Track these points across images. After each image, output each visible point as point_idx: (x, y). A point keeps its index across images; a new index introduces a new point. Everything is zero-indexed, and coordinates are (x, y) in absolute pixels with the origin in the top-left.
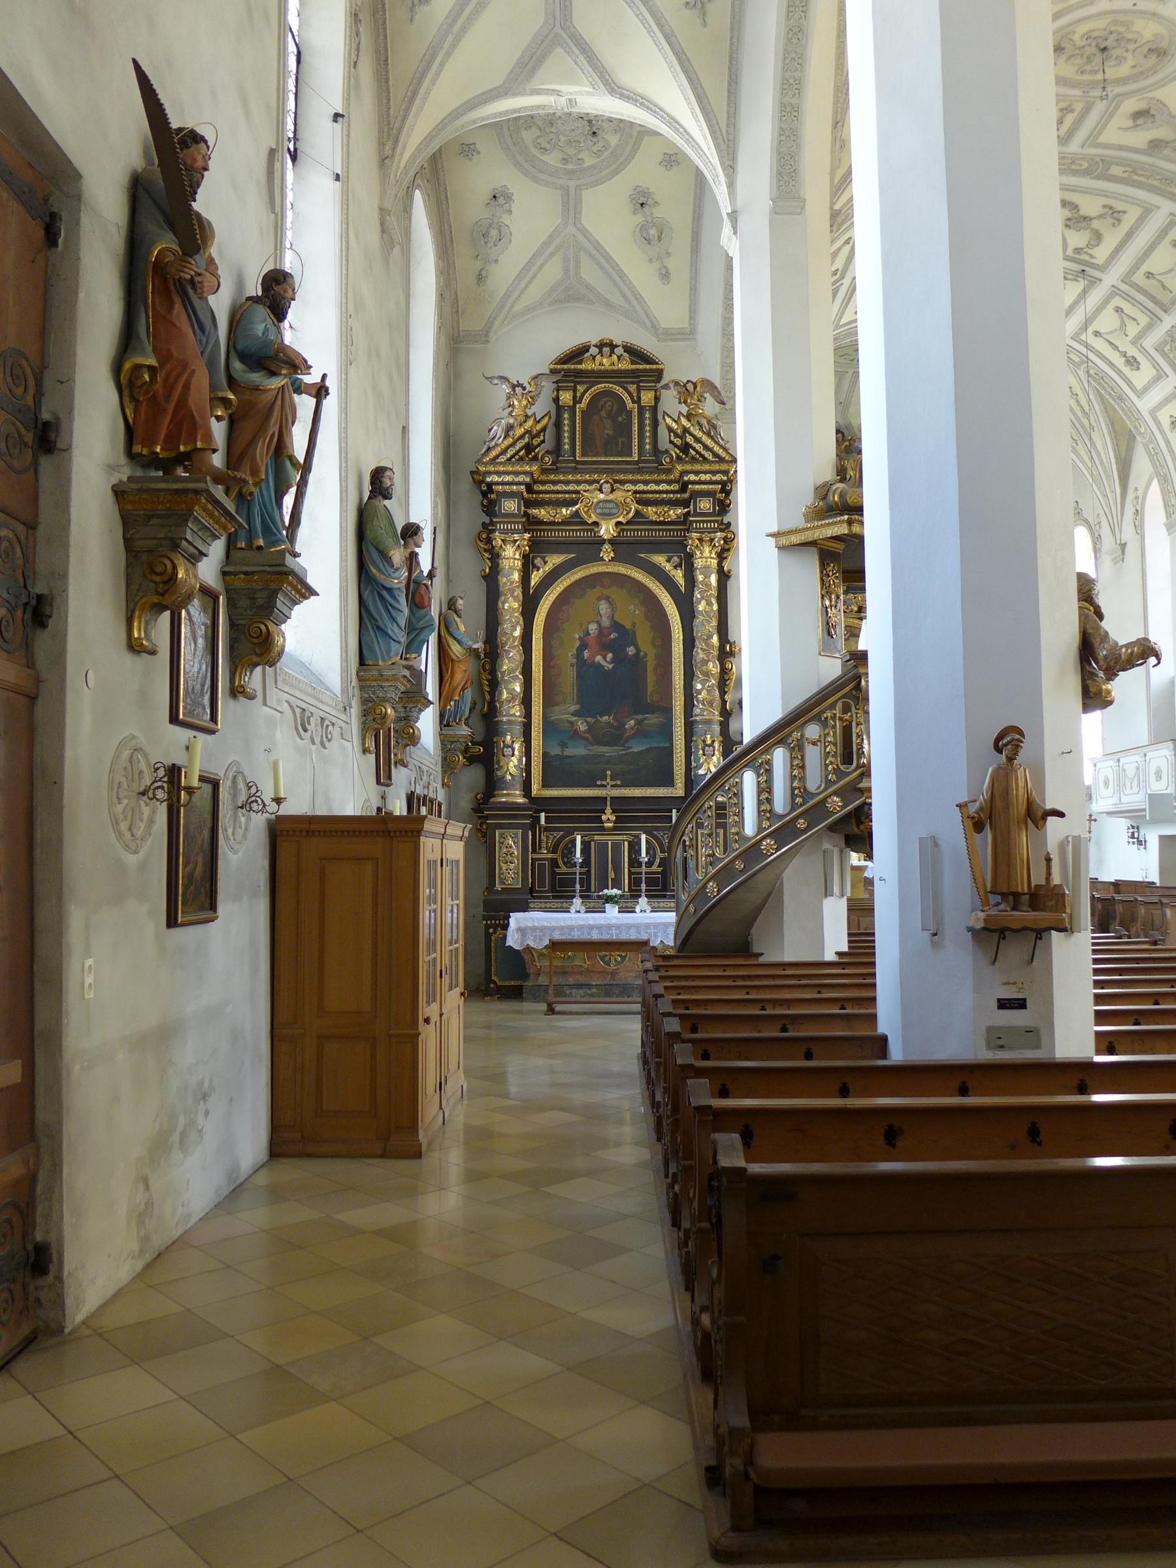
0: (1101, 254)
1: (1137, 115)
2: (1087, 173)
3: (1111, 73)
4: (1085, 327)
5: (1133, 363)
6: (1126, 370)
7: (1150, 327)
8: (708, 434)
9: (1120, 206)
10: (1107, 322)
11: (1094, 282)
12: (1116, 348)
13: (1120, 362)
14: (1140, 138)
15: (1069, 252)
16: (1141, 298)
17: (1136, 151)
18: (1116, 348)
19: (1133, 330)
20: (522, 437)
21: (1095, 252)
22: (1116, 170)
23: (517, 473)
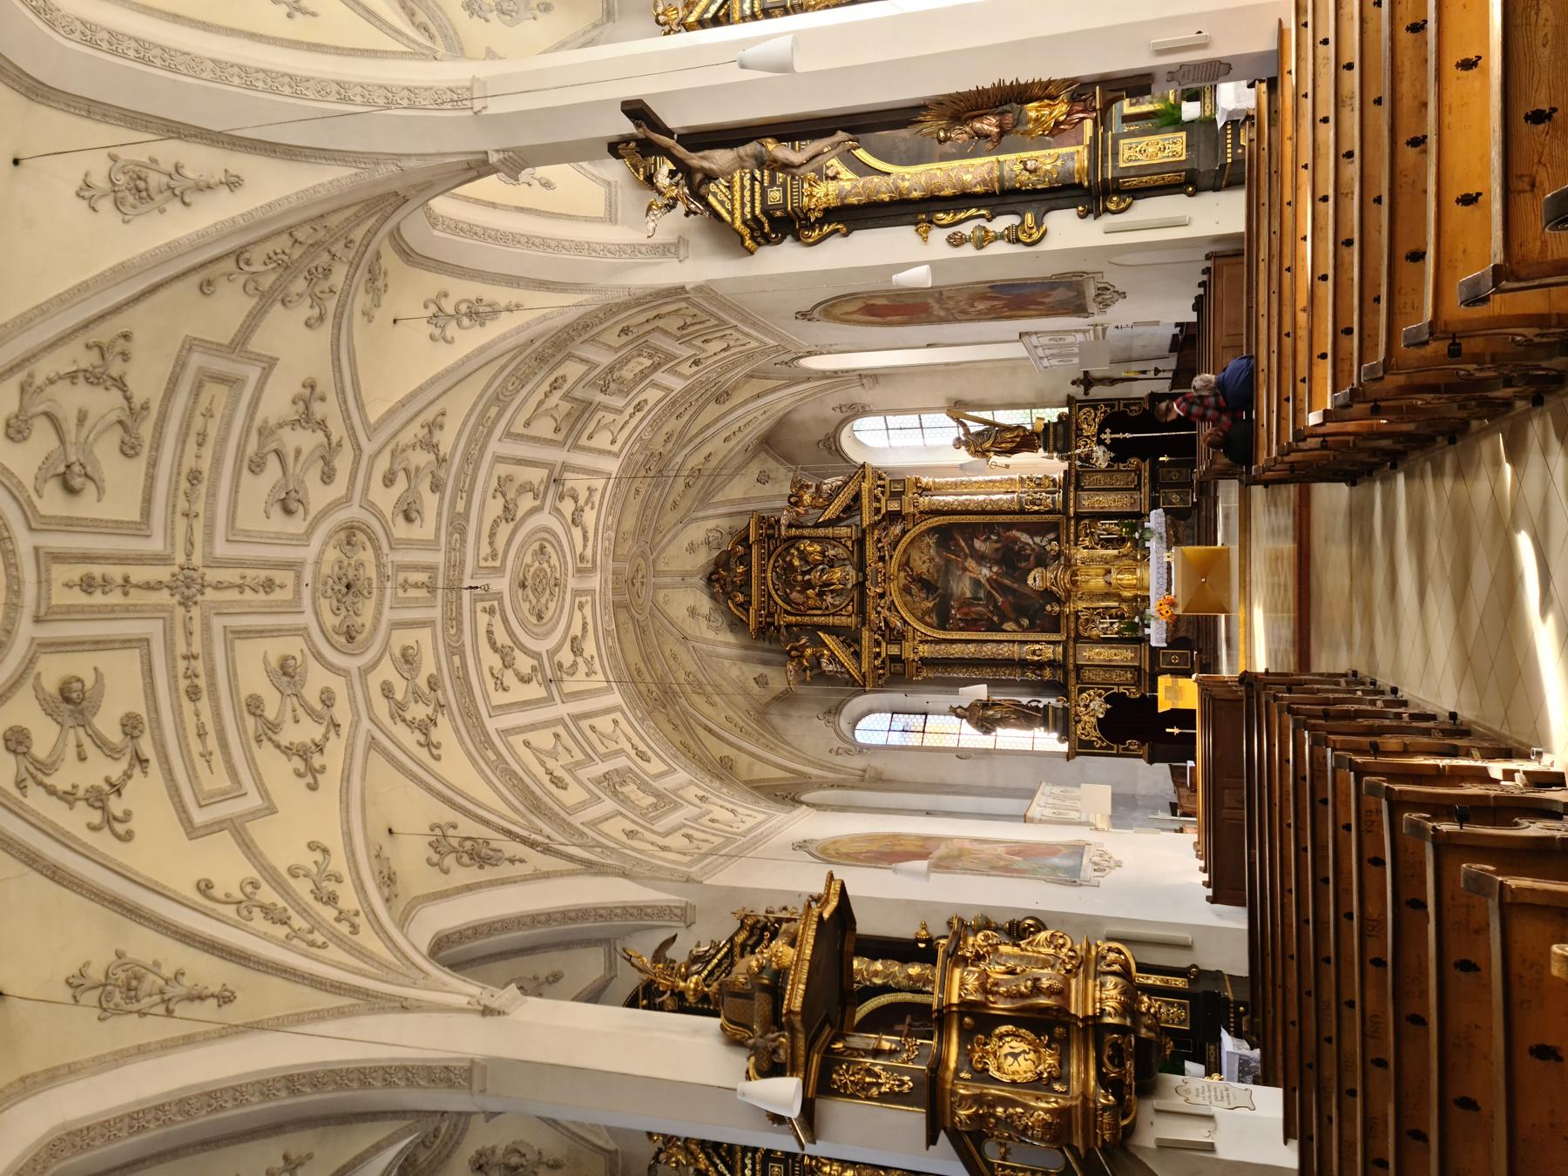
0: (537, 476)
1: (408, 519)
2: (463, 532)
3: (371, 571)
4: (609, 452)
5: (638, 408)
6: (646, 409)
7: (606, 408)
8: (709, 962)
9: (494, 484)
10: (602, 440)
11: (566, 467)
12: (626, 423)
13: (639, 415)
14: (430, 501)
15: (538, 503)
16: (579, 426)
17: (442, 499)
18: (626, 423)
19: (610, 417)
20: (708, 1157)
21: (536, 483)
22: (460, 506)
23: (744, 1166)
